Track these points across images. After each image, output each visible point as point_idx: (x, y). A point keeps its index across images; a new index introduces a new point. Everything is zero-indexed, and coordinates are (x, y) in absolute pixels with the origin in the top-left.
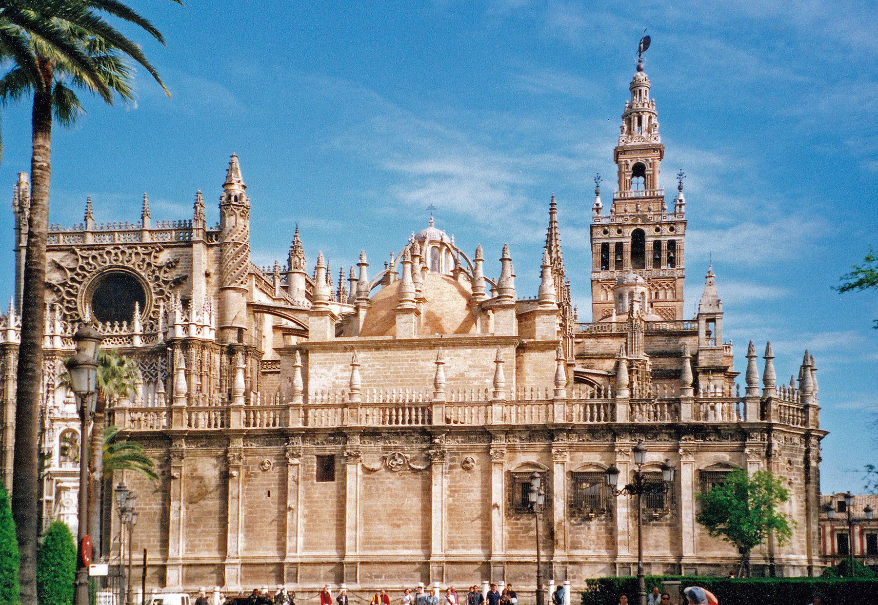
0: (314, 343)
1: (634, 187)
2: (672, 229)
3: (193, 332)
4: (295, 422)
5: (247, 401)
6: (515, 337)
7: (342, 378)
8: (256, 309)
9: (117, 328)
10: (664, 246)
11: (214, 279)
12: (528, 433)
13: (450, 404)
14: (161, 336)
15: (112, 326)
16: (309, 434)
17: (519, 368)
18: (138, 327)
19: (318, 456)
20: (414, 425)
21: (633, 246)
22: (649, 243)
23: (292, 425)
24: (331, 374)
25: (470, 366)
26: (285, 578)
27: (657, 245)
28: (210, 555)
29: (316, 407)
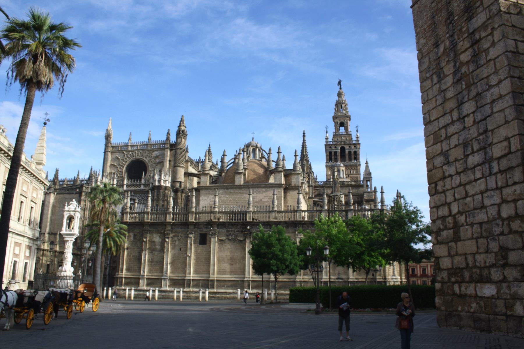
0: (202, 187)
1: (341, 131)
2: (355, 147)
3: (162, 183)
4: (192, 219)
5: (173, 210)
6: (283, 184)
8: (188, 175)
9: (136, 182)
10: (352, 153)
11: (172, 163)
13: (254, 212)
14: (151, 185)
15: (134, 181)
16: (196, 225)
17: (285, 198)
18: (143, 181)
19: (201, 234)
20: (239, 221)
21: (341, 152)
22: (347, 151)
23: (190, 220)
24: (208, 199)
25: (265, 197)
26: (186, 285)
27: (350, 152)
28: (155, 275)
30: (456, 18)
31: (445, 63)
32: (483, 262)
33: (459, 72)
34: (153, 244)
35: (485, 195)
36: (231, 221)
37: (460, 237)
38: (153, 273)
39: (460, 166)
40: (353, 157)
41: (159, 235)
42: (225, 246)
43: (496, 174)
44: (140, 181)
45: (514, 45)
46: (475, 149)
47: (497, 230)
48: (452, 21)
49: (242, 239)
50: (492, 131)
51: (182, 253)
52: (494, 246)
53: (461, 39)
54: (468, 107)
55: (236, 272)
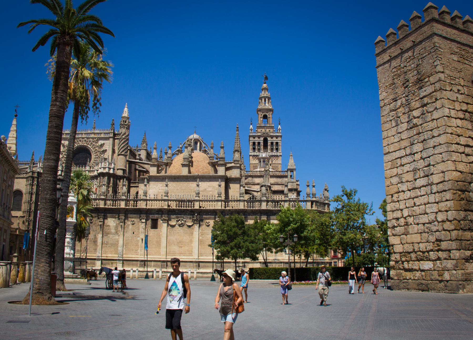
7: (161, 189)
12: (230, 212)
18: (88, 168)
20: (188, 208)
25: (209, 186)
27: (272, 143)
29: (152, 200)
30: (410, 85)
31: (402, 114)
32: (424, 248)
33: (411, 122)
34: (108, 227)
35: (427, 206)
36: (180, 208)
37: (409, 232)
38: (108, 254)
39: (410, 185)
40: (274, 147)
41: (114, 219)
42: (175, 230)
43: (435, 193)
44: (85, 167)
45: (448, 112)
46: (421, 176)
47: (434, 229)
48: (408, 86)
49: (190, 224)
50: (433, 165)
51: (135, 237)
52: (432, 239)
53: (414, 100)
54: (418, 147)
55: (185, 253)
